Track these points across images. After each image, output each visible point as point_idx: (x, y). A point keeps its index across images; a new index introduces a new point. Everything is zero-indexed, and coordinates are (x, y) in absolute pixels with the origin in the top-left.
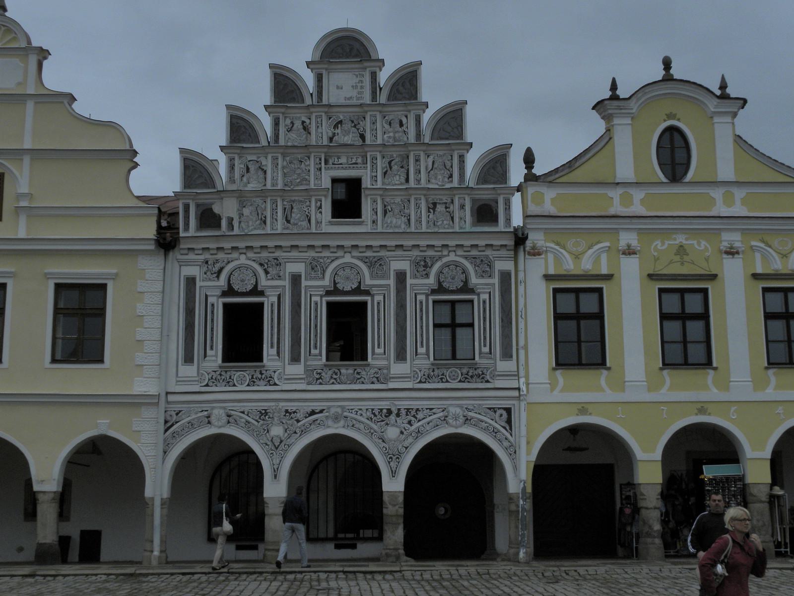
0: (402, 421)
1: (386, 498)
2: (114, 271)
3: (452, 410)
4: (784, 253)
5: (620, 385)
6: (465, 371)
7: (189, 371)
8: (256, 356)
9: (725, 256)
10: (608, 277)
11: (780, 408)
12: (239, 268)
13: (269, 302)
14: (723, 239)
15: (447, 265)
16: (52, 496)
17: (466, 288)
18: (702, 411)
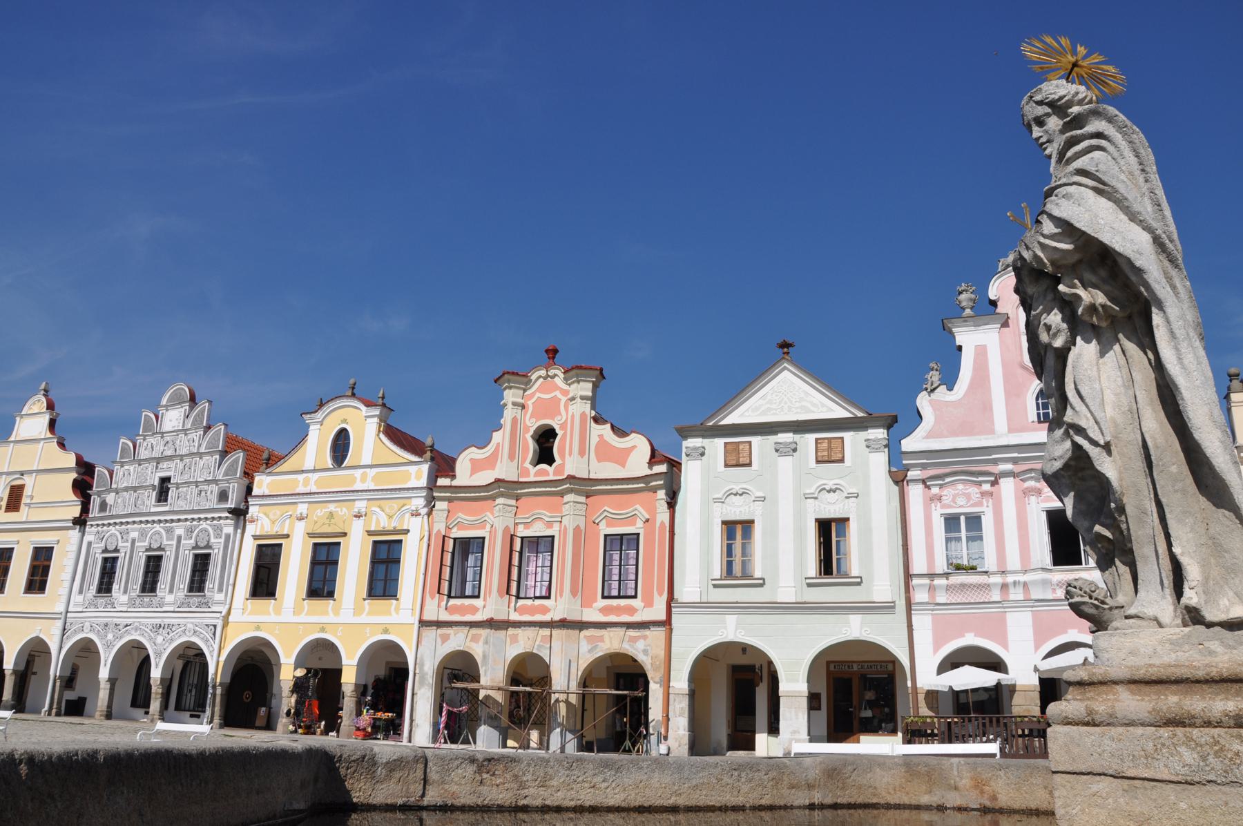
0: (165, 632)
1: (152, 682)
2: (57, 539)
3: (190, 626)
4: (391, 515)
5: (278, 611)
6: (199, 600)
7: (77, 598)
8: (109, 590)
9: (354, 518)
10: (287, 536)
11: (368, 629)
12: (111, 535)
13: (121, 555)
14: (356, 506)
15: (201, 531)
16: (11, 671)
17: (208, 546)
18: (323, 630)
